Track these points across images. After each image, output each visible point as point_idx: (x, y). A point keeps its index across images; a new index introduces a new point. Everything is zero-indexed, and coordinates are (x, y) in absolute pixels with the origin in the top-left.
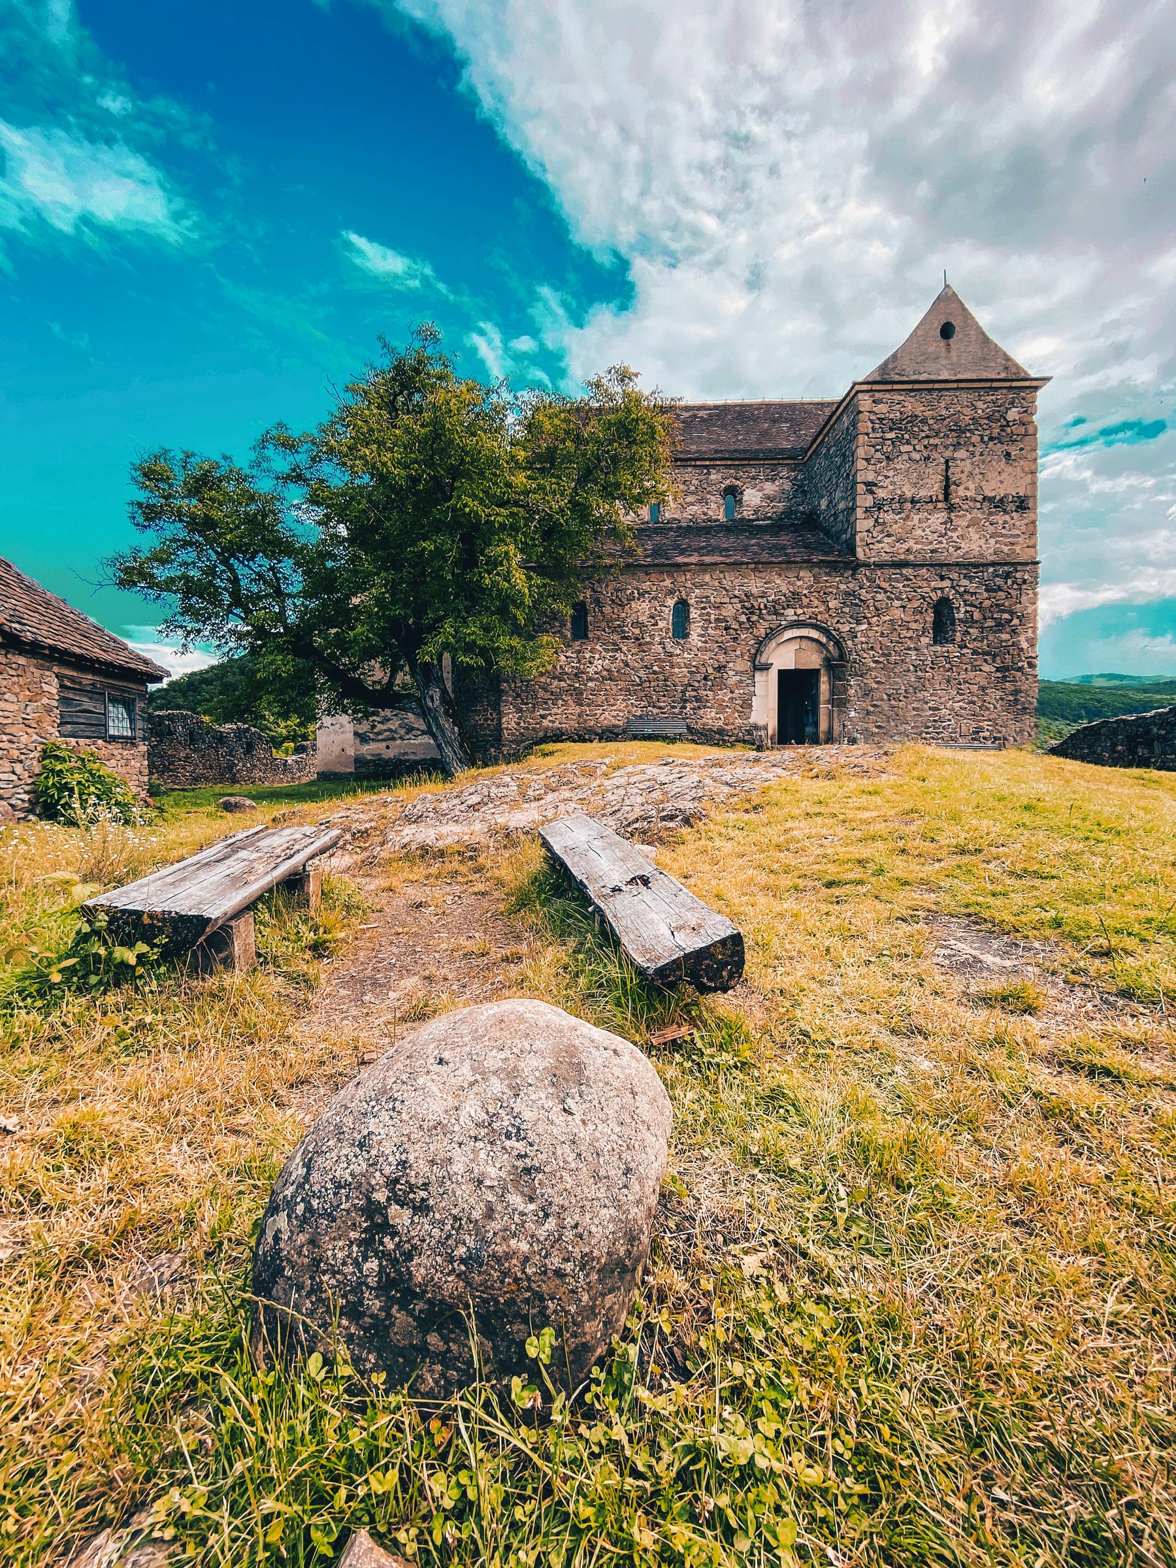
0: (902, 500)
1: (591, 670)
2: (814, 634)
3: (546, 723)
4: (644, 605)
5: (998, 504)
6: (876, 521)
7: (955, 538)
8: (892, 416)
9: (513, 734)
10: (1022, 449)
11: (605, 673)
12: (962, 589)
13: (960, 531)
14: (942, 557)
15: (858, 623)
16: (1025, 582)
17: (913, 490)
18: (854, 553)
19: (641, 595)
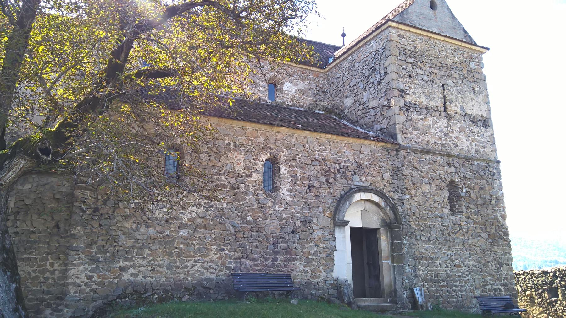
1: (185, 217)
2: (376, 198)
3: (126, 276)
4: (240, 157)
5: (473, 121)
7: (453, 138)
8: (410, 48)
9: (81, 291)
10: (480, 88)
11: (199, 221)
12: (462, 175)
13: (455, 135)
14: (448, 150)
15: (403, 192)
16: (494, 174)
17: (427, 101)
18: (396, 139)
19: (237, 147)
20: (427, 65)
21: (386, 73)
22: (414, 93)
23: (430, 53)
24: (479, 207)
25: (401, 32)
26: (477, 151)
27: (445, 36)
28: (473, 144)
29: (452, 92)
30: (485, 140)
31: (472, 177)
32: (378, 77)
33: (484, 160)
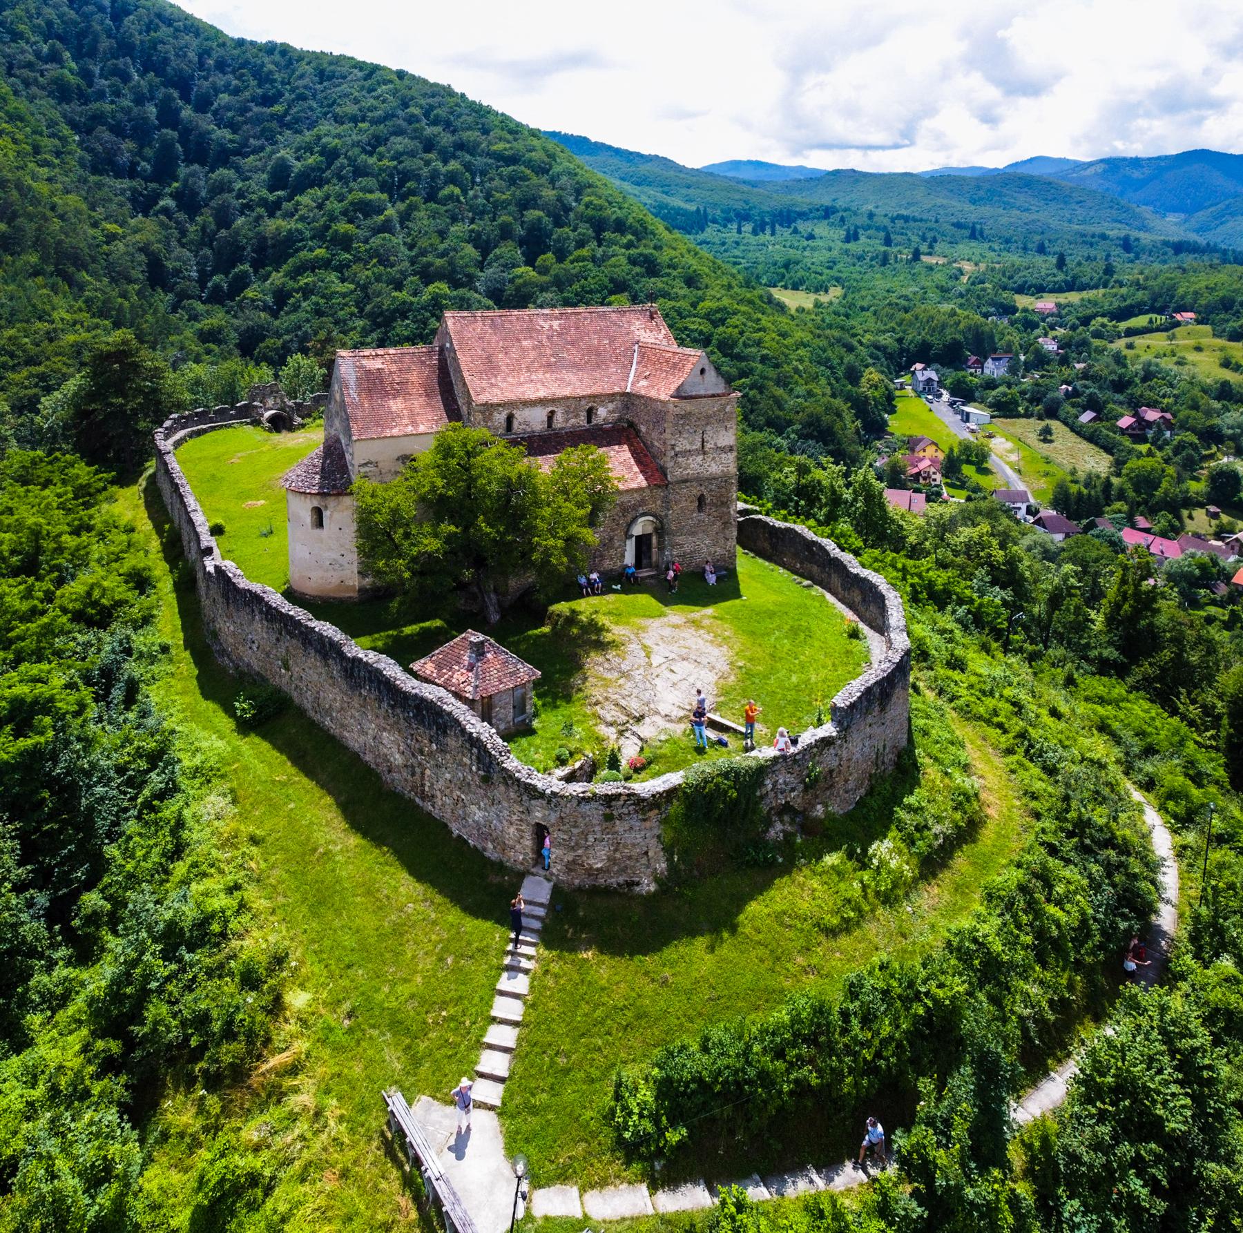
0: (686, 451)
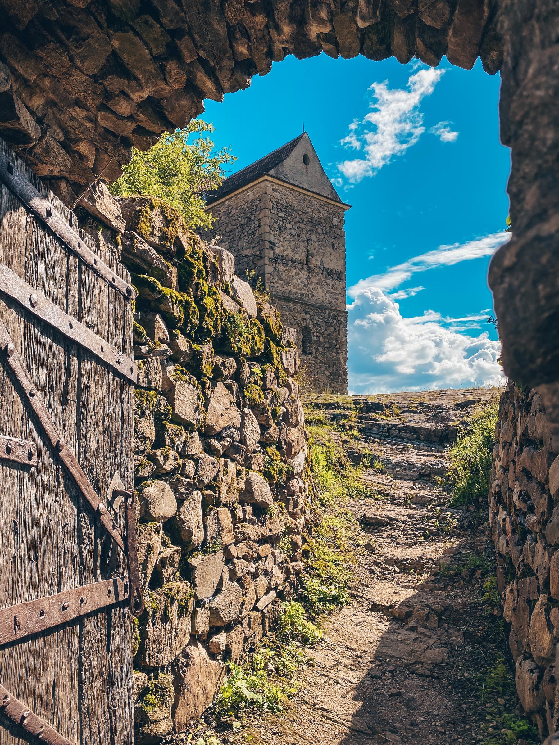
5: (330, 274)
6: (275, 268)
8: (282, 202)
10: (339, 244)
14: (306, 299)
17: (293, 253)
20: (296, 220)
21: (260, 226)
22: (283, 246)
23: (299, 208)
24: (326, 350)
25: (276, 186)
26: (330, 302)
27: (314, 193)
28: (327, 295)
29: (314, 246)
30: (337, 292)
31: (323, 324)
32: (253, 227)
33: (334, 310)
